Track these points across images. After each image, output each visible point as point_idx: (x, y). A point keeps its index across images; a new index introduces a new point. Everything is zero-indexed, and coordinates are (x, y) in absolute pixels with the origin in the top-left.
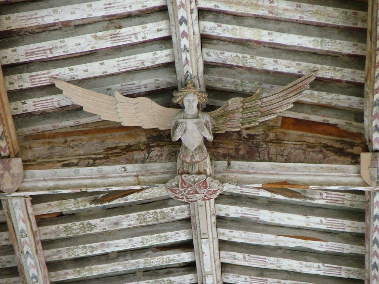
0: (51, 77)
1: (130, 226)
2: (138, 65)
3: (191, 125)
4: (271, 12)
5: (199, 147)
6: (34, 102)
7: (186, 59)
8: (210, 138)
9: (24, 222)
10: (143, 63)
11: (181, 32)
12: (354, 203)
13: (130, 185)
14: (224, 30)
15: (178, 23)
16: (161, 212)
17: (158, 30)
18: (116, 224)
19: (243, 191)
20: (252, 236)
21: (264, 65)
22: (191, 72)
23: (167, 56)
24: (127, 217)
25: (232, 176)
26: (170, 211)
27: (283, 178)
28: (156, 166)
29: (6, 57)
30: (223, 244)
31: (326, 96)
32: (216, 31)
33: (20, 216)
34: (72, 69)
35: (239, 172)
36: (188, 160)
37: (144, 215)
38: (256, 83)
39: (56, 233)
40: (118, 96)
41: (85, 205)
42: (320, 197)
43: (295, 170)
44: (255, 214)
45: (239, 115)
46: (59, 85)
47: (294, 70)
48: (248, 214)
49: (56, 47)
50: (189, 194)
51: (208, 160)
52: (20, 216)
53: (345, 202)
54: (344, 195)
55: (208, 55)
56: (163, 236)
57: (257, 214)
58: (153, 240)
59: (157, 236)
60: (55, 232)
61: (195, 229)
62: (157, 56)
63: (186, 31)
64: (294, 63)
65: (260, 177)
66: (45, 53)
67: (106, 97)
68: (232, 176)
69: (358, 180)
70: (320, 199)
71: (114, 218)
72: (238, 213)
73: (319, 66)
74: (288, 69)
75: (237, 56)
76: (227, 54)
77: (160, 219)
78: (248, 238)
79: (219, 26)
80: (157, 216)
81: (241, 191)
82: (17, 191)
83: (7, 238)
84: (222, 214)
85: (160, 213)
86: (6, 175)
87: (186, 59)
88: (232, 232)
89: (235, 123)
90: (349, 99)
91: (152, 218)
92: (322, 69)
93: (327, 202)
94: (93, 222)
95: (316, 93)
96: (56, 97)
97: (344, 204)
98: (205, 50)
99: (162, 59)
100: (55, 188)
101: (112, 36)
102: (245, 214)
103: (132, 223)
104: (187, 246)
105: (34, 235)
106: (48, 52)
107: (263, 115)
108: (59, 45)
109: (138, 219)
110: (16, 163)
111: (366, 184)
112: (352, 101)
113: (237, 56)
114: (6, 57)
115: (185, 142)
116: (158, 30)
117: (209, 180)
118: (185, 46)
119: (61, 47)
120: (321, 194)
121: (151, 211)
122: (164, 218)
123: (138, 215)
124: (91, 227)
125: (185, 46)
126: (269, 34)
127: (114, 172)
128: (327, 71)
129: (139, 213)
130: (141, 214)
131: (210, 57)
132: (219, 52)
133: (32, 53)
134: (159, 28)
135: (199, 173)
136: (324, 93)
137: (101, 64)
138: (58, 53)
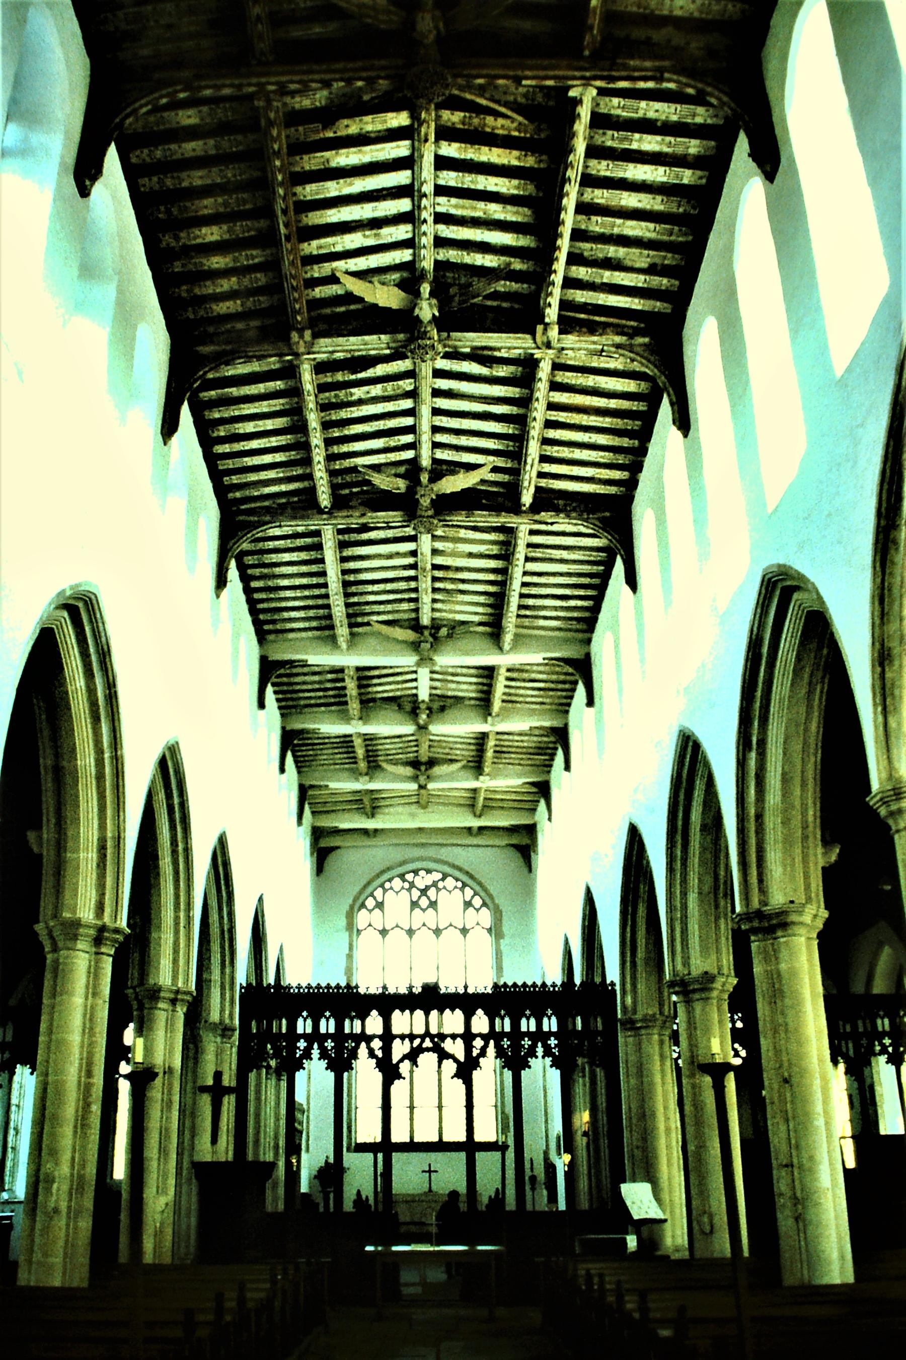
0: (333, 270)
3: (425, 305)
4: (485, 213)
5: (430, 322)
8: (437, 314)
13: (382, 349)
17: (407, 232)
18: (368, 392)
25: (450, 343)
27: (484, 344)
28: (401, 336)
30: (436, 412)
35: (455, 340)
36: (423, 329)
40: (376, 283)
43: (491, 338)
45: (457, 299)
46: (338, 274)
47: (494, 264)
51: (435, 331)
58: (390, 407)
60: (327, 398)
64: (496, 258)
65: (468, 343)
67: (368, 284)
68: (450, 343)
69: (533, 345)
71: (366, 388)
73: (512, 260)
76: (451, 252)
82: (309, 353)
84: (436, 386)
86: (301, 342)
89: (454, 304)
94: (353, 390)
95: (508, 283)
96: (335, 287)
100: (333, 352)
101: (376, 235)
104: (411, 412)
105: (316, 396)
107: (474, 297)
110: (308, 334)
111: (538, 348)
115: (421, 317)
116: (407, 232)
117: (436, 344)
124: (352, 394)
127: (373, 340)
135: (430, 339)
138: (339, 248)
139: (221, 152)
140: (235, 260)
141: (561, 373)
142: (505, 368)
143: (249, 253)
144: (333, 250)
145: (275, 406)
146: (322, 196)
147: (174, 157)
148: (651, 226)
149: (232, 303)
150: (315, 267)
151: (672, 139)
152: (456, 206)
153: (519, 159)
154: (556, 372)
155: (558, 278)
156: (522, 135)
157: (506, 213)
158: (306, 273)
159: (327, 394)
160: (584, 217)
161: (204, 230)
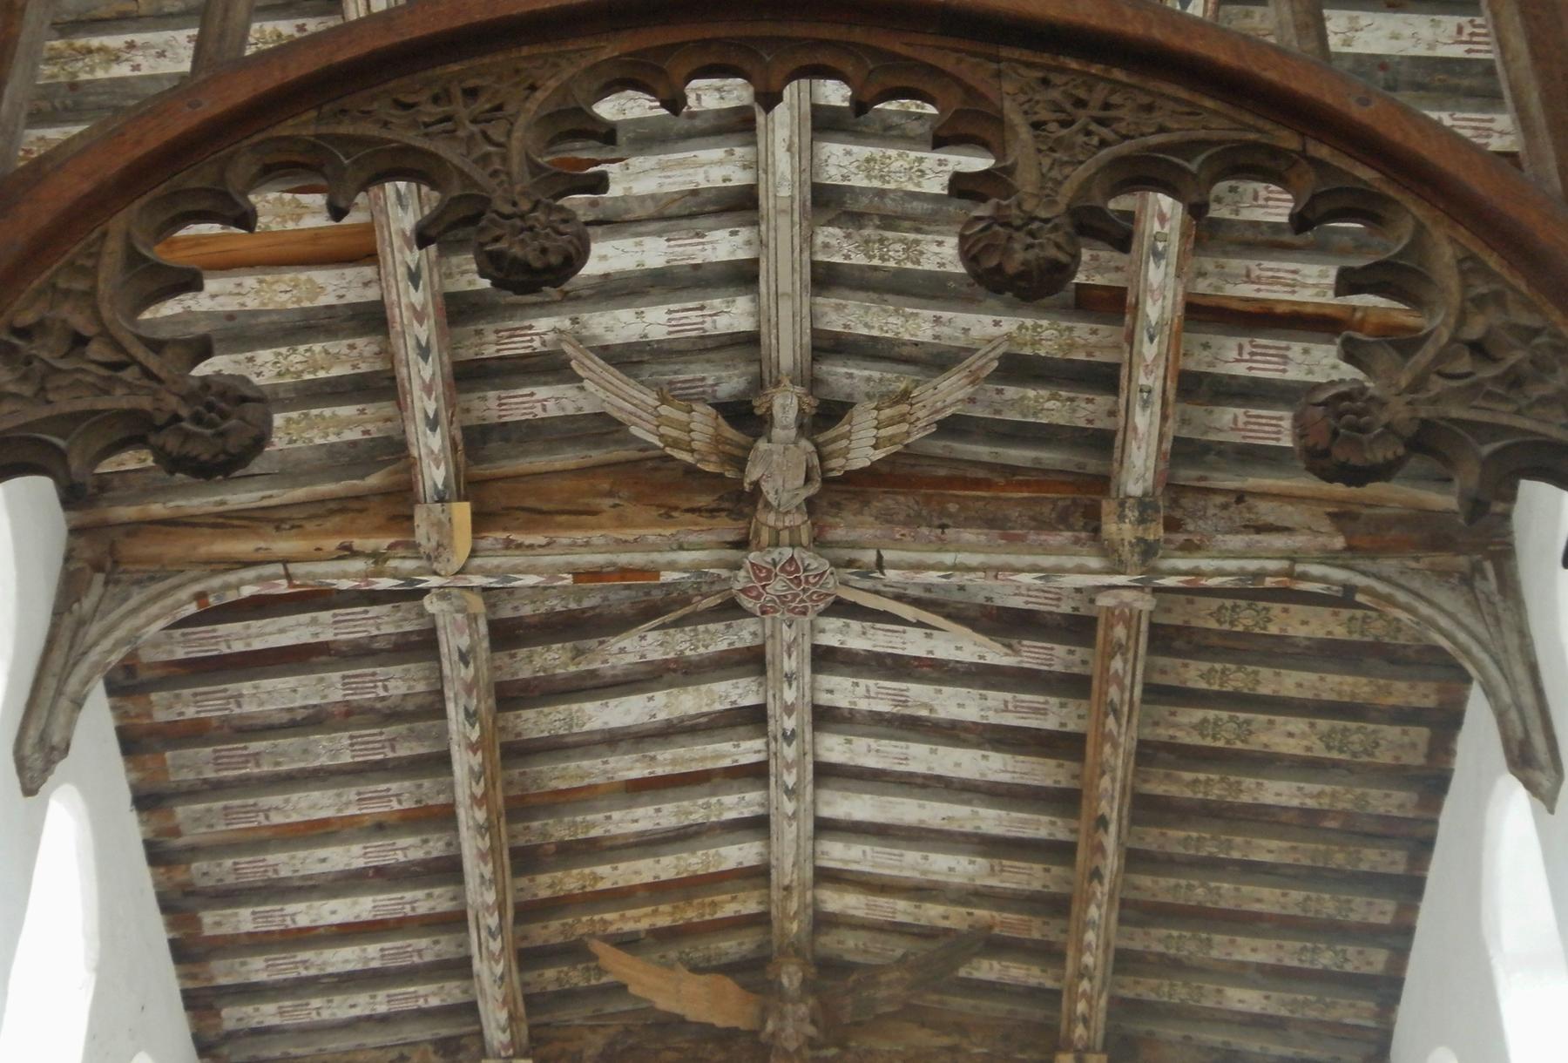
1: (940, 238)
2: (872, 631)
4: (653, 758)
6: (1058, 606)
7: (790, 656)
9: (1135, 429)
10: (864, 633)
11: (794, 717)
12: (476, 340)
14: (726, 697)
15: (799, 731)
16: (871, 257)
19: (700, 313)
20: (681, 179)
21: (661, 645)
22: (785, 627)
23: (823, 631)
24: (943, 265)
26: (853, 256)
29: (1080, 717)
31: (555, 602)
32: (739, 691)
33: (1139, 448)
34: (981, 657)
37: (907, 258)
38: (675, 595)
39: (1095, 264)
41: (1021, 327)
42: (545, 337)
44: (677, 249)
48: (690, 244)
49: (996, 711)
50: (795, 596)
52: (1139, 448)
53: (493, 337)
54: (498, 351)
55: (754, 634)
56: (875, 177)
57: (670, 250)
59: (888, 182)
61: (804, 205)
62: (839, 637)
63: (785, 718)
66: (1016, 707)
70: (544, 334)
72: (711, 242)
73: (572, 669)
74: (622, 645)
75: (706, 647)
77: (874, 242)
78: (691, 171)
79: (733, 703)
80: (880, 249)
81: (705, 312)
83: (1200, 280)
85: (874, 256)
87: (790, 656)
88: (724, 181)
90: (516, 608)
91: (891, 247)
92: (566, 665)
93: (531, 327)
95: (573, 606)
97: (497, 332)
98: (758, 642)
99: (832, 626)
102: (698, 244)
103: (935, 248)
106: (1010, 707)
108: (991, 714)
109: (922, 253)
112: (510, 606)
113: (706, 647)
114: (1080, 717)
116: (831, 692)
118: (790, 685)
119: (989, 709)
120: (544, 343)
121: (892, 264)
122: (867, 242)
123: (918, 263)
125: (790, 685)
126: (654, 716)
128: (557, 662)
129: (916, 267)
130: (913, 263)
131: (752, 629)
132: (738, 645)
133: (1036, 711)
134: (829, 696)
136: (559, 608)
137: (931, 652)
138: (996, 697)
139: (1204, 936)
140: (1246, 731)
141: (364, 368)
142: (537, 343)
143: (1209, 742)
144: (1008, 696)
145: (1275, 281)
146: (1014, 815)
147: (1298, 945)
148: (276, 819)
149: (1291, 632)
150: (1058, 667)
151: (304, 973)
152: (722, 756)
153: (596, 878)
154: (378, 366)
155: (469, 817)
156: (597, 917)
157: (605, 772)
158: (1084, 662)
159: (1098, 280)
160: (431, 803)
161: (1295, 802)
